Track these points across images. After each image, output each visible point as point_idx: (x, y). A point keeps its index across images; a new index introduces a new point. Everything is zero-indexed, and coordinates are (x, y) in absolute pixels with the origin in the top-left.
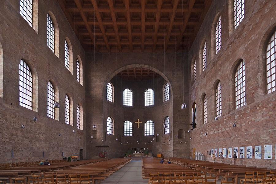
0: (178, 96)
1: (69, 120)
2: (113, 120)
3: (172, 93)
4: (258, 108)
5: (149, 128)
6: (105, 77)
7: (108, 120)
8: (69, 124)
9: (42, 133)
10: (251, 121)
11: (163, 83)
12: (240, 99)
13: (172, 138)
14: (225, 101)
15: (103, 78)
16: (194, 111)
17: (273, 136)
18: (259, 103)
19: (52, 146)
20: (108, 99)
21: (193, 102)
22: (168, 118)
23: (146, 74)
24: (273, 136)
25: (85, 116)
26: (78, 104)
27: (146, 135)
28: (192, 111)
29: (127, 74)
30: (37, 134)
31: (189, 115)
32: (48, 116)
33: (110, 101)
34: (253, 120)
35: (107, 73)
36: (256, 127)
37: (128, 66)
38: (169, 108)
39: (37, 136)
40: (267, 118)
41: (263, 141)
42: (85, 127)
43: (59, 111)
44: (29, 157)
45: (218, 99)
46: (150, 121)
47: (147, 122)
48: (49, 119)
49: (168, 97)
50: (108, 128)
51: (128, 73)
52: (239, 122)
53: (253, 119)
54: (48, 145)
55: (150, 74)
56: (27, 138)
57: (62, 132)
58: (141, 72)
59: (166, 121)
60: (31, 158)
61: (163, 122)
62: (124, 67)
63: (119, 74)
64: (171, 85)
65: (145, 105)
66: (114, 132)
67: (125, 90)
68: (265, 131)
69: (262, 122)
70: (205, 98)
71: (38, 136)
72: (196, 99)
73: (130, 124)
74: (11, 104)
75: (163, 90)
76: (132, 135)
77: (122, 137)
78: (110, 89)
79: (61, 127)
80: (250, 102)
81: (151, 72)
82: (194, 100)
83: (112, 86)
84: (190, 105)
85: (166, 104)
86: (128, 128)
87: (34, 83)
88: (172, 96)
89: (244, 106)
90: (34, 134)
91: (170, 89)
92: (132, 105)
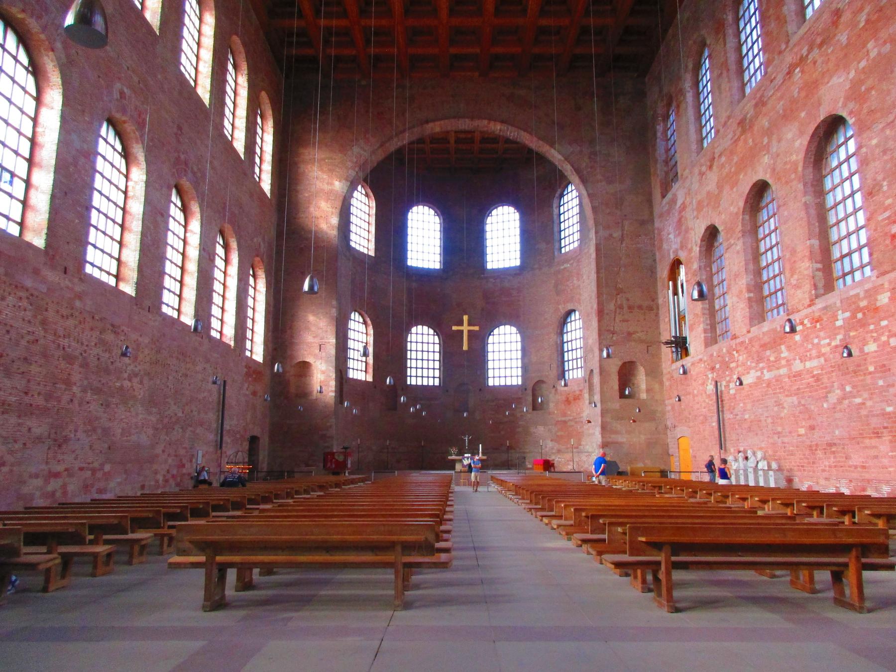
0: (615, 235)
1: (223, 326)
2: (369, 322)
3: (591, 223)
5: (505, 357)
6: (349, 164)
7: (352, 325)
9: (142, 373)
11: (554, 184)
12: (849, 254)
16: (675, 293)
20: (353, 244)
21: (672, 257)
22: (577, 316)
25: (272, 309)
27: (491, 383)
28: (671, 292)
30: (126, 375)
31: (658, 308)
33: (362, 250)
38: (578, 280)
39: (127, 384)
44: (96, 465)
45: (767, 251)
46: (508, 327)
47: (496, 331)
49: (577, 236)
56: (98, 391)
57: (199, 368)
60: (102, 465)
64: (589, 195)
65: (489, 266)
66: (371, 370)
67: (415, 209)
71: (129, 384)
73: (431, 337)
74: (66, 268)
75: (556, 211)
78: (363, 208)
80: (886, 267)
82: (676, 251)
83: (367, 195)
84: (659, 269)
85: (567, 261)
86: (424, 356)
87: (130, 194)
89: (864, 280)
90: (118, 379)
91: (581, 205)
92: (437, 266)
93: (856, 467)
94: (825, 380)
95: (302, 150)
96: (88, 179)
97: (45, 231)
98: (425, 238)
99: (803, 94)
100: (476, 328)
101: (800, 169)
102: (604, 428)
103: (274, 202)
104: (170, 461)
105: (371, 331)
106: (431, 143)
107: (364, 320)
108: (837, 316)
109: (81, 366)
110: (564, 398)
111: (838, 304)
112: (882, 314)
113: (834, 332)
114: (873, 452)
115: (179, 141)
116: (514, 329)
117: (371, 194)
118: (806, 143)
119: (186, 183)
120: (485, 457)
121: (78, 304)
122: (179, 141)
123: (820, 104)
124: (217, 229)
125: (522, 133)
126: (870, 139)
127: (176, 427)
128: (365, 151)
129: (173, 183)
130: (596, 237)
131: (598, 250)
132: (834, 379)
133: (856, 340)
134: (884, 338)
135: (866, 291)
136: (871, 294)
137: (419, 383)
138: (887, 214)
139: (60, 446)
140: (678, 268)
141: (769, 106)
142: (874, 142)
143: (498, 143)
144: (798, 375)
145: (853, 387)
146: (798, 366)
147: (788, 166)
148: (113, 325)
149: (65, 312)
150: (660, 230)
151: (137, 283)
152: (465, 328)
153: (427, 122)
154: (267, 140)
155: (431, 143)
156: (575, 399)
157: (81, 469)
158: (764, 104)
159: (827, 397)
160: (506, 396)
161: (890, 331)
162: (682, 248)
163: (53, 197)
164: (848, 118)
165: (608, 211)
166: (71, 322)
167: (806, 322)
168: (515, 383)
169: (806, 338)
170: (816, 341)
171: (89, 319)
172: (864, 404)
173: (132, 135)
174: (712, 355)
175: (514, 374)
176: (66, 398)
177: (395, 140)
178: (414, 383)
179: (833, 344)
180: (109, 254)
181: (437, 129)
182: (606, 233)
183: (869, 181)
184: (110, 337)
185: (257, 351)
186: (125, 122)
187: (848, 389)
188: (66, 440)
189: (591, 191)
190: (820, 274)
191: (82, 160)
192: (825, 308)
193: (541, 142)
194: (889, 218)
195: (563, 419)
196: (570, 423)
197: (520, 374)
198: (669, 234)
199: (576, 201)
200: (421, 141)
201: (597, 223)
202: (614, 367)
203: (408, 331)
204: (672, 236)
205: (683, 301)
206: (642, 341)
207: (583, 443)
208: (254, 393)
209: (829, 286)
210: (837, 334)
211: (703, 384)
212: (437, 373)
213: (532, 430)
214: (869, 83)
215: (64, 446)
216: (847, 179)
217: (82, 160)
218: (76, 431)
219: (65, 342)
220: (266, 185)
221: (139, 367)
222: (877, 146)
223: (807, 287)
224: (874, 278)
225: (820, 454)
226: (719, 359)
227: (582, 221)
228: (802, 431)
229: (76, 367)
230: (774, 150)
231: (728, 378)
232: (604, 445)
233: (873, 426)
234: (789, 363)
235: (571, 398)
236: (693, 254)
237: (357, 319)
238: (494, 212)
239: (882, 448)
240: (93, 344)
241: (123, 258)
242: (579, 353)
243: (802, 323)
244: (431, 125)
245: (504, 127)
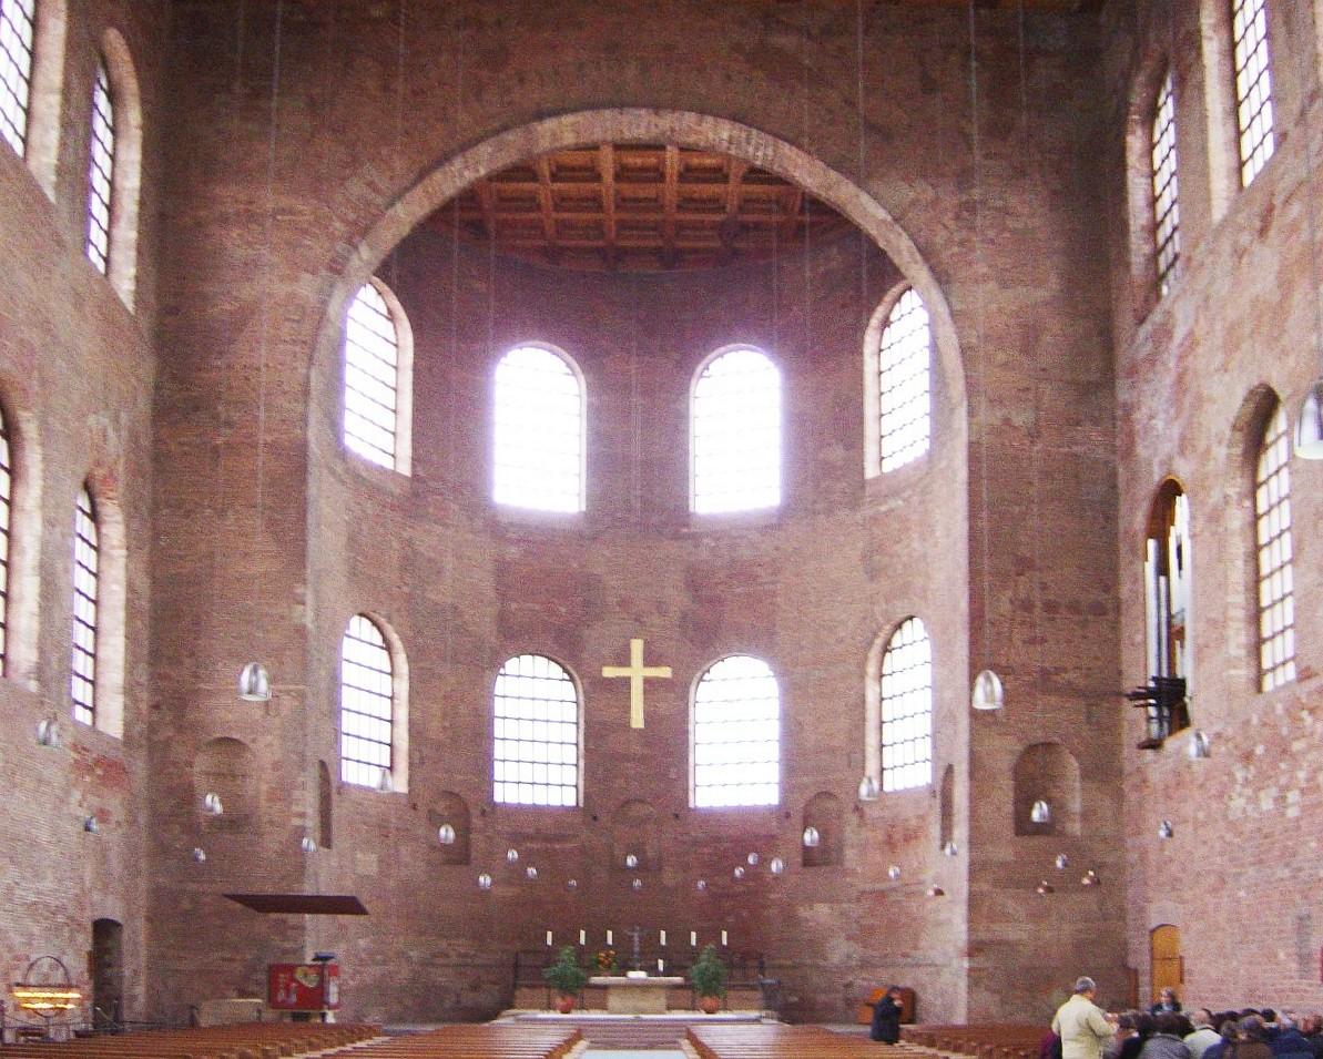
0: (1018, 420)
3: (958, 388)
13: (961, 831)
15: (315, 236)
23: (716, 204)
26: (87, 487)
28: (1150, 567)
29: (539, 208)
35: (356, 188)
37: (550, 124)
49: (925, 426)
51: (545, 190)
55: (747, 203)
58: (671, 190)
62: (510, 137)
63: (469, 198)
64: (953, 314)
70: (1270, 437)
72: (1185, 446)
77: (477, 822)
78: (373, 340)
81: (757, 189)
88: (962, 411)
95: (218, 190)
103: (145, 323)
106: (555, 178)
110: (880, 836)
130: (970, 424)
131: (974, 459)
143: (725, 179)
150: (1129, 409)
154: (119, 162)
156: (907, 839)
160: (735, 838)
162: (1182, 452)
165: (1001, 357)
174: (1247, 723)
189: (958, 307)
195: (878, 886)
196: (893, 897)
198: (1151, 417)
201: (972, 388)
204: (1159, 424)
205: (1181, 585)
206: (1072, 691)
207: (923, 944)
211: (1220, 796)
220: (125, 283)
226: (1266, 731)
231: (1283, 780)
232: (974, 949)
236: (1211, 466)
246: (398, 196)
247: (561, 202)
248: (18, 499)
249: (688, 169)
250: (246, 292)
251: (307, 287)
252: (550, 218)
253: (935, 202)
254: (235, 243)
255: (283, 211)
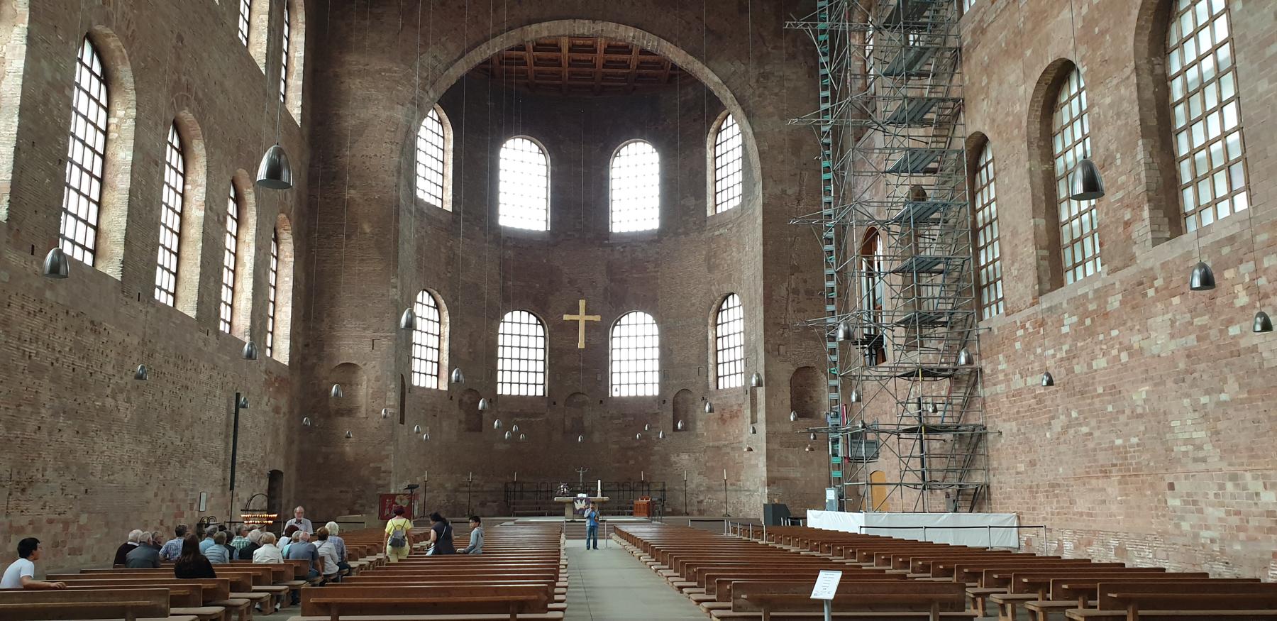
0: (789, 192)
1: (237, 316)
3: (757, 173)
4: (1151, 293)
5: (635, 358)
8: (227, 331)
9: (129, 386)
10: (1128, 348)
14: (1016, 241)
15: (403, 85)
16: (870, 274)
17: (1220, 426)
18: (1152, 269)
19: (159, 452)
20: (420, 194)
23: (625, 65)
24: (1221, 426)
25: (302, 287)
29: (525, 64)
30: (109, 391)
32: (157, 297)
33: (432, 201)
34: (1136, 346)
36: (1152, 378)
39: (109, 402)
40: (1191, 340)
41: (1183, 449)
42: (300, 346)
43: (202, 266)
44: (69, 515)
46: (641, 314)
47: (624, 320)
48: (158, 310)
49: (738, 190)
50: (417, 351)
51: (529, 56)
52: (1082, 349)
53: (1136, 340)
54: (144, 450)
55: (641, 65)
57: (203, 377)
58: (600, 57)
59: (724, 317)
60: (78, 516)
61: (711, 321)
68: (1186, 402)
69: (1172, 359)
75: (710, 154)
76: (540, 393)
78: (433, 143)
79: (200, 349)
80: (1117, 262)
81: (648, 58)
83: (440, 122)
85: (724, 225)
86: (522, 355)
91: (744, 146)
93: (1081, 514)
94: (1048, 403)
96: (61, 121)
97: (8, 197)
98: (524, 185)
99: (1029, 26)
100: (597, 318)
101: (1024, 124)
102: (769, 457)
103: (305, 131)
104: (164, 508)
105: (446, 318)
106: (535, 50)
107: (436, 303)
108: (1062, 320)
109: (52, 380)
111: (1065, 305)
112: (1113, 322)
113: (1059, 340)
114: (1099, 496)
115: (179, 58)
116: (649, 318)
117: (447, 121)
118: (1031, 91)
119: (187, 116)
120: (606, 498)
121: (48, 294)
122: (179, 58)
123: (1048, 43)
124: (229, 178)
125: (664, 42)
126: (1104, 96)
127: (173, 462)
128: (440, 62)
129: (171, 118)
132: (1059, 401)
133: (1084, 353)
134: (1115, 352)
135: (1096, 291)
136: (1102, 294)
137: (515, 393)
138: (1120, 195)
139: (23, 490)
140: (874, 240)
141: (989, 35)
142: (1108, 100)
143: (630, 52)
144: (1019, 393)
145: (1080, 412)
146: (1018, 383)
147: (1010, 119)
148: (92, 322)
149: (31, 307)
151: (123, 262)
152: (582, 318)
153: (530, 23)
155: (535, 50)
157: (51, 522)
158: (983, 31)
159: (1050, 424)
161: (1120, 343)
163: (17, 150)
164: (1079, 66)
165: (781, 157)
166: (38, 321)
167: (1028, 325)
168: (649, 393)
169: (1028, 347)
170: (1039, 351)
171: (62, 316)
172: (1091, 434)
173: (117, 53)
175: (649, 380)
176: (32, 425)
177: (484, 46)
178: (507, 392)
179: (1058, 356)
180: (87, 224)
181: (545, 34)
182: (778, 190)
183: (1101, 150)
184: (89, 339)
185: (282, 351)
186: (107, 36)
187: (1074, 414)
188: (31, 482)
190: (1046, 263)
191: (54, 97)
192: (1050, 309)
193: (690, 57)
194: (1121, 200)
195: (716, 444)
197: (657, 380)
199: (738, 140)
200: (521, 48)
202: (785, 372)
203: (498, 318)
208: (276, 410)
209: (1058, 282)
210: (1062, 344)
212: (540, 378)
213: (673, 458)
214: (1103, 24)
215: (29, 491)
216: (1079, 142)
217: (54, 97)
218: (44, 469)
219: (31, 348)
220: (295, 107)
221: (126, 379)
222: (1111, 106)
223: (1031, 278)
224: (1104, 275)
225: (1041, 497)
227: (746, 169)
228: (1021, 467)
229: (46, 380)
230: (993, 94)
232: (771, 482)
233: (1101, 462)
234: (1008, 380)
235: (727, 415)
237: (426, 302)
238: (624, 151)
239: (1109, 490)
240: (67, 349)
241: (104, 226)
242: (739, 353)
243: (1023, 327)
244: (534, 27)
245: (639, 33)
246: (451, 64)
247: (538, 62)
248: (241, 236)
249: (609, 46)
250: (364, 114)
251: (400, 114)
252: (531, 69)
253: (747, 71)
254: (356, 87)
255: (384, 70)
